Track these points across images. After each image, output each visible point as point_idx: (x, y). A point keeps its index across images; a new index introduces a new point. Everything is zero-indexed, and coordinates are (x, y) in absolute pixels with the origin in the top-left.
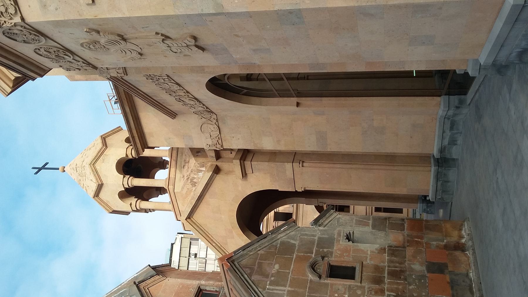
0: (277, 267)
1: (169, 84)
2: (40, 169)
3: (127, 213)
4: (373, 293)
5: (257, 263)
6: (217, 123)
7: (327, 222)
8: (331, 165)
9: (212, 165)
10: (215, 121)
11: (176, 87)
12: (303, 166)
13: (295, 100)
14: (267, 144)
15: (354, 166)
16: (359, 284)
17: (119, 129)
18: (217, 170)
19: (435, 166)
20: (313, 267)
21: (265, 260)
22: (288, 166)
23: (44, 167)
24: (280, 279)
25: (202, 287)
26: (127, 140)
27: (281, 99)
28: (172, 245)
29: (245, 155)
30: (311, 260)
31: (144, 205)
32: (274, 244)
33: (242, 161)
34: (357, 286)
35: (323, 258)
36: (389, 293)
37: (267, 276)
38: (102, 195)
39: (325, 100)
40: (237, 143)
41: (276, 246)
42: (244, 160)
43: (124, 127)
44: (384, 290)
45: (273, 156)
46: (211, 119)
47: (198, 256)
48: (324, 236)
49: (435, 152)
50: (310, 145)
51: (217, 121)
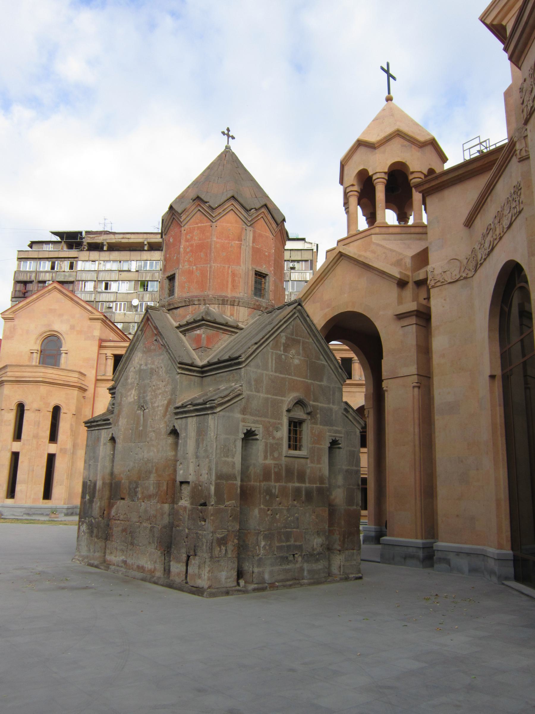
0: (296, 362)
1: (510, 215)
2: (387, 72)
3: (341, 182)
4: (276, 470)
5: (299, 338)
6: (462, 278)
7: (350, 417)
8: (417, 421)
9: (408, 276)
10: (464, 275)
11: (506, 222)
12: (414, 387)
13: (498, 372)
14: (439, 342)
15: (417, 449)
16: (284, 454)
17: (444, 159)
18: (402, 284)
19: (423, 543)
20: (300, 403)
21: (304, 349)
22: (413, 369)
23: (390, 76)
24: (283, 366)
25: (267, 278)
26: (431, 171)
27: (498, 355)
28: (303, 239)
29: (423, 317)
30: (307, 400)
31: (353, 201)
32: (322, 357)
33: (415, 313)
34: (282, 452)
35: (309, 414)
36: (277, 487)
37: (285, 351)
38: (362, 150)
39: (500, 411)
40: (438, 305)
41: (319, 359)
42: (417, 316)
43: (447, 166)
44: (280, 482)
45: (425, 350)
46: (466, 270)
47: (292, 271)
48: (334, 414)
49: (440, 544)
50: (441, 394)
51: (465, 278)
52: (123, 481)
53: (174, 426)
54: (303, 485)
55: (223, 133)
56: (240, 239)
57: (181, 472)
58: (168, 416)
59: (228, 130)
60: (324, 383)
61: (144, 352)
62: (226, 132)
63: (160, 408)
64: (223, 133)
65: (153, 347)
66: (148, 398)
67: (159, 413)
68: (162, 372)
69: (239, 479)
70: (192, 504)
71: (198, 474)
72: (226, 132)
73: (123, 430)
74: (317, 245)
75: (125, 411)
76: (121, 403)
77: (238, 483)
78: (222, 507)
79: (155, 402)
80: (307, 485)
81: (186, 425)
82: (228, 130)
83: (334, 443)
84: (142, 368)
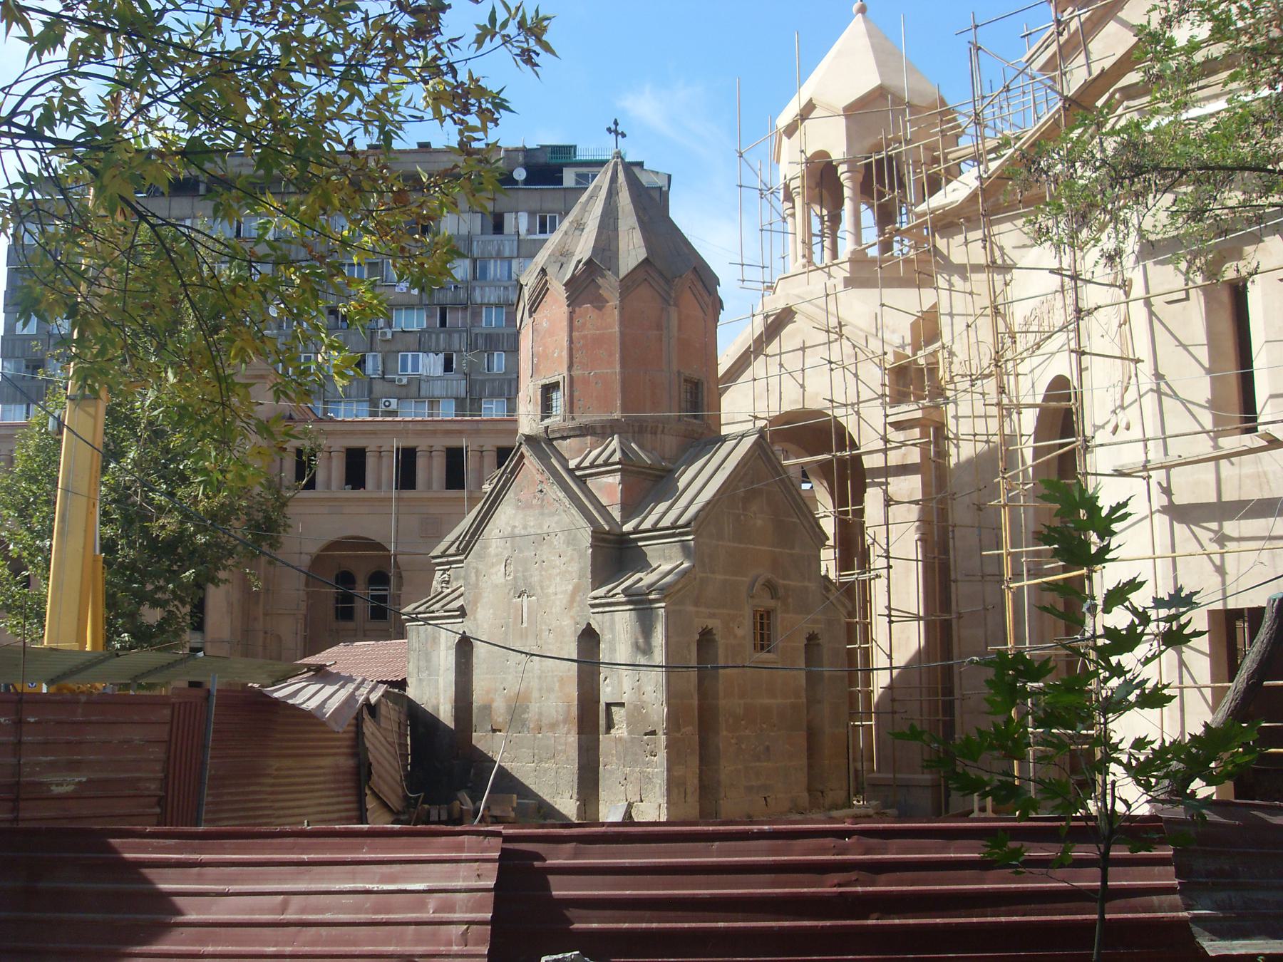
0: (759, 523)
52: (495, 705)
53: (589, 624)
54: (773, 701)
55: (609, 130)
56: (659, 327)
57: (608, 689)
58: (576, 609)
59: (616, 123)
60: (796, 551)
61: (518, 507)
62: (613, 127)
63: (559, 596)
64: (609, 130)
65: (535, 501)
66: (536, 579)
67: (558, 603)
68: (558, 542)
69: (696, 697)
70: (630, 733)
71: (639, 690)
72: (613, 127)
73: (485, 626)
74: (669, 176)
75: (487, 596)
76: (477, 584)
77: (695, 702)
78: (679, 735)
79: (548, 587)
80: (780, 701)
81: (613, 622)
82: (616, 123)
83: (812, 638)
84: (517, 531)
